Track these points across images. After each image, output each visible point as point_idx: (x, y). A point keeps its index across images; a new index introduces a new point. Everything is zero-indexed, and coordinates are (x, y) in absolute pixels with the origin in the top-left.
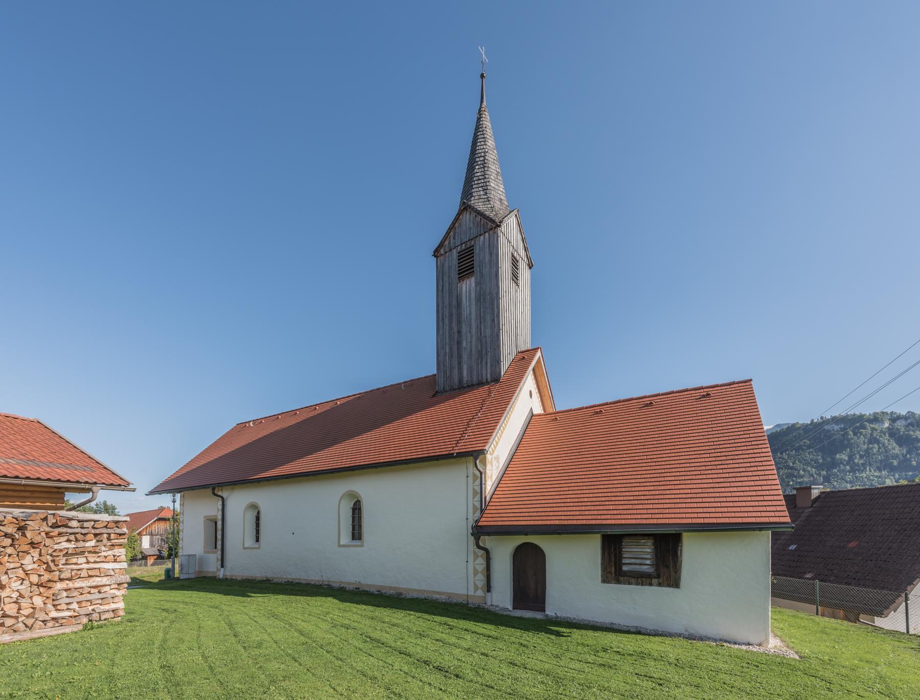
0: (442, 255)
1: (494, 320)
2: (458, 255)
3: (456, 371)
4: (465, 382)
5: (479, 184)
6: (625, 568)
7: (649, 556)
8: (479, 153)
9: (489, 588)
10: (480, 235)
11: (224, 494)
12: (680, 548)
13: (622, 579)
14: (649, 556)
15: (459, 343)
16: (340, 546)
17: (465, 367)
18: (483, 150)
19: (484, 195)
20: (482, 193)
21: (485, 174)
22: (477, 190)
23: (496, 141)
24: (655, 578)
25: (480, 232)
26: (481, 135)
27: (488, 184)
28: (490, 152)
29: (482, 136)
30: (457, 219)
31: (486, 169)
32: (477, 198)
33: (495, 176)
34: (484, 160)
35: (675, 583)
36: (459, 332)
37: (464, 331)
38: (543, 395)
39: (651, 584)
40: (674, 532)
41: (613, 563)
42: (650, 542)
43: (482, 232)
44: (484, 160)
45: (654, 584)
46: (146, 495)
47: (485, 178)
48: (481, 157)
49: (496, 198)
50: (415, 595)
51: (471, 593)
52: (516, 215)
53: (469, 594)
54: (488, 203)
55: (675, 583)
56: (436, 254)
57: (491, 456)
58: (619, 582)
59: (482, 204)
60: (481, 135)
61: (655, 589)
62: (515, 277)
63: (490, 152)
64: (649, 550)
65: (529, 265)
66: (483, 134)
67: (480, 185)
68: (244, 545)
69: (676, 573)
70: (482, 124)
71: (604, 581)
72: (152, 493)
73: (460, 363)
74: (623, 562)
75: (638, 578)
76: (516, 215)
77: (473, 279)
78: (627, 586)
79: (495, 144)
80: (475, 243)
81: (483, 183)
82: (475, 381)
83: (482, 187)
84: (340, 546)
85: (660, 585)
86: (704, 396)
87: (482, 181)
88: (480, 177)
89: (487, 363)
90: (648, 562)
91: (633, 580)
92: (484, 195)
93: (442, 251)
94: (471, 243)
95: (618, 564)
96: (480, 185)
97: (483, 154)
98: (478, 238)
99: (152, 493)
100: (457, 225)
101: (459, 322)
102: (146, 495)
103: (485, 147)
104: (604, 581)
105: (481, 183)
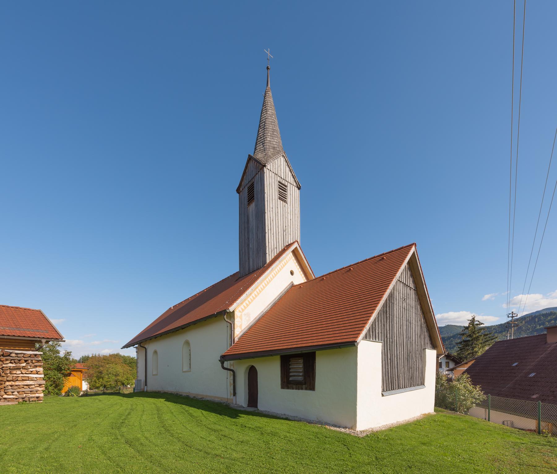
0: (241, 191)
2: (248, 189)
6: (291, 379)
7: (301, 371)
9: (235, 394)
10: (257, 174)
12: (315, 364)
15: (248, 245)
16: (183, 372)
17: (251, 260)
22: (259, 145)
24: (304, 384)
25: (256, 172)
26: (264, 108)
27: (265, 139)
29: (265, 109)
31: (265, 130)
32: (258, 150)
33: (271, 133)
34: (265, 124)
35: (312, 387)
36: (248, 238)
37: (250, 237)
39: (302, 389)
40: (300, 352)
42: (301, 361)
43: (257, 172)
44: (265, 124)
45: (304, 389)
46: (122, 348)
48: (263, 122)
49: (270, 147)
50: (208, 399)
51: (229, 397)
52: (283, 156)
54: (264, 152)
55: (312, 387)
57: (241, 313)
58: (288, 388)
59: (261, 153)
60: (264, 108)
62: (283, 197)
63: (269, 118)
64: (301, 366)
65: (297, 187)
66: (266, 107)
71: (283, 387)
72: (124, 347)
73: (249, 259)
75: (297, 385)
76: (283, 156)
82: (255, 268)
84: (183, 372)
85: (306, 389)
86: (380, 260)
87: (263, 138)
88: (261, 136)
89: (260, 256)
90: (301, 374)
91: (294, 386)
97: (264, 121)
99: (124, 347)
100: (247, 171)
101: (248, 232)
102: (122, 348)
104: (283, 387)
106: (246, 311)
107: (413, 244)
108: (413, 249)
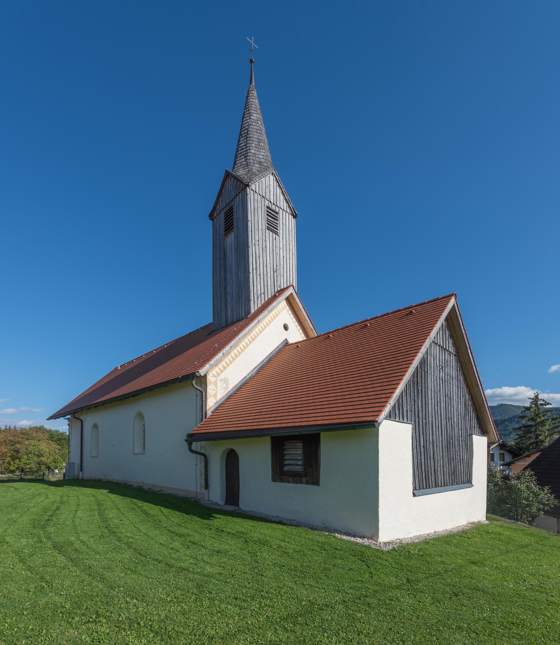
0: (215, 217)
1: (246, 265)
2: (224, 215)
3: (224, 312)
4: (229, 321)
5: (242, 152)
6: (286, 469)
7: (300, 458)
8: (244, 127)
9: (207, 486)
10: (237, 196)
11: (82, 418)
12: (319, 449)
13: (284, 478)
14: (300, 457)
15: (225, 288)
16: (135, 454)
17: (229, 308)
18: (248, 124)
19: (245, 161)
20: (243, 160)
21: (247, 144)
22: (240, 158)
23: (264, 113)
24: (304, 477)
25: (237, 193)
26: (247, 111)
27: (248, 151)
28: (254, 124)
29: (248, 112)
30: (223, 186)
31: (248, 139)
32: (239, 165)
33: (257, 143)
34: (247, 132)
35: (316, 482)
36: (225, 279)
37: (228, 278)
38: (306, 328)
39: (301, 483)
40: (298, 433)
41: (278, 464)
42: (300, 445)
43: (238, 193)
44: (247, 132)
45: (304, 483)
46: (48, 419)
47: (247, 147)
48: (245, 129)
49: (255, 162)
50: (170, 492)
51: (199, 491)
52: (273, 173)
53: (197, 491)
54: (247, 167)
55: (316, 482)
56: (211, 218)
57: (215, 378)
58: (282, 481)
59: (242, 169)
60: (247, 111)
61: (304, 486)
62: (272, 227)
63: (254, 124)
64: (300, 452)
65: (293, 215)
66: (249, 110)
67: (243, 154)
68: (91, 455)
69: (317, 472)
70: (249, 102)
71: (274, 480)
72: (51, 418)
73: (226, 306)
74: (285, 463)
75: (294, 477)
76: (273, 173)
77: (233, 234)
78: (287, 484)
79: (263, 116)
80: (234, 203)
81: (245, 151)
82: (235, 320)
83: (244, 155)
84: (135, 454)
85: (307, 483)
86: (407, 315)
87: (245, 150)
88: (243, 147)
89: (242, 303)
90: (300, 463)
91: (291, 479)
92: (245, 161)
93: (215, 215)
94: (231, 204)
95: (282, 465)
96: (243, 154)
97: (247, 127)
98: (235, 199)
99: (51, 418)
100: (223, 191)
101: (225, 271)
102: (48, 419)
103: (249, 121)
104: (274, 480)
105: (244, 152)
106: (222, 376)
107: (452, 295)
108: (452, 301)
